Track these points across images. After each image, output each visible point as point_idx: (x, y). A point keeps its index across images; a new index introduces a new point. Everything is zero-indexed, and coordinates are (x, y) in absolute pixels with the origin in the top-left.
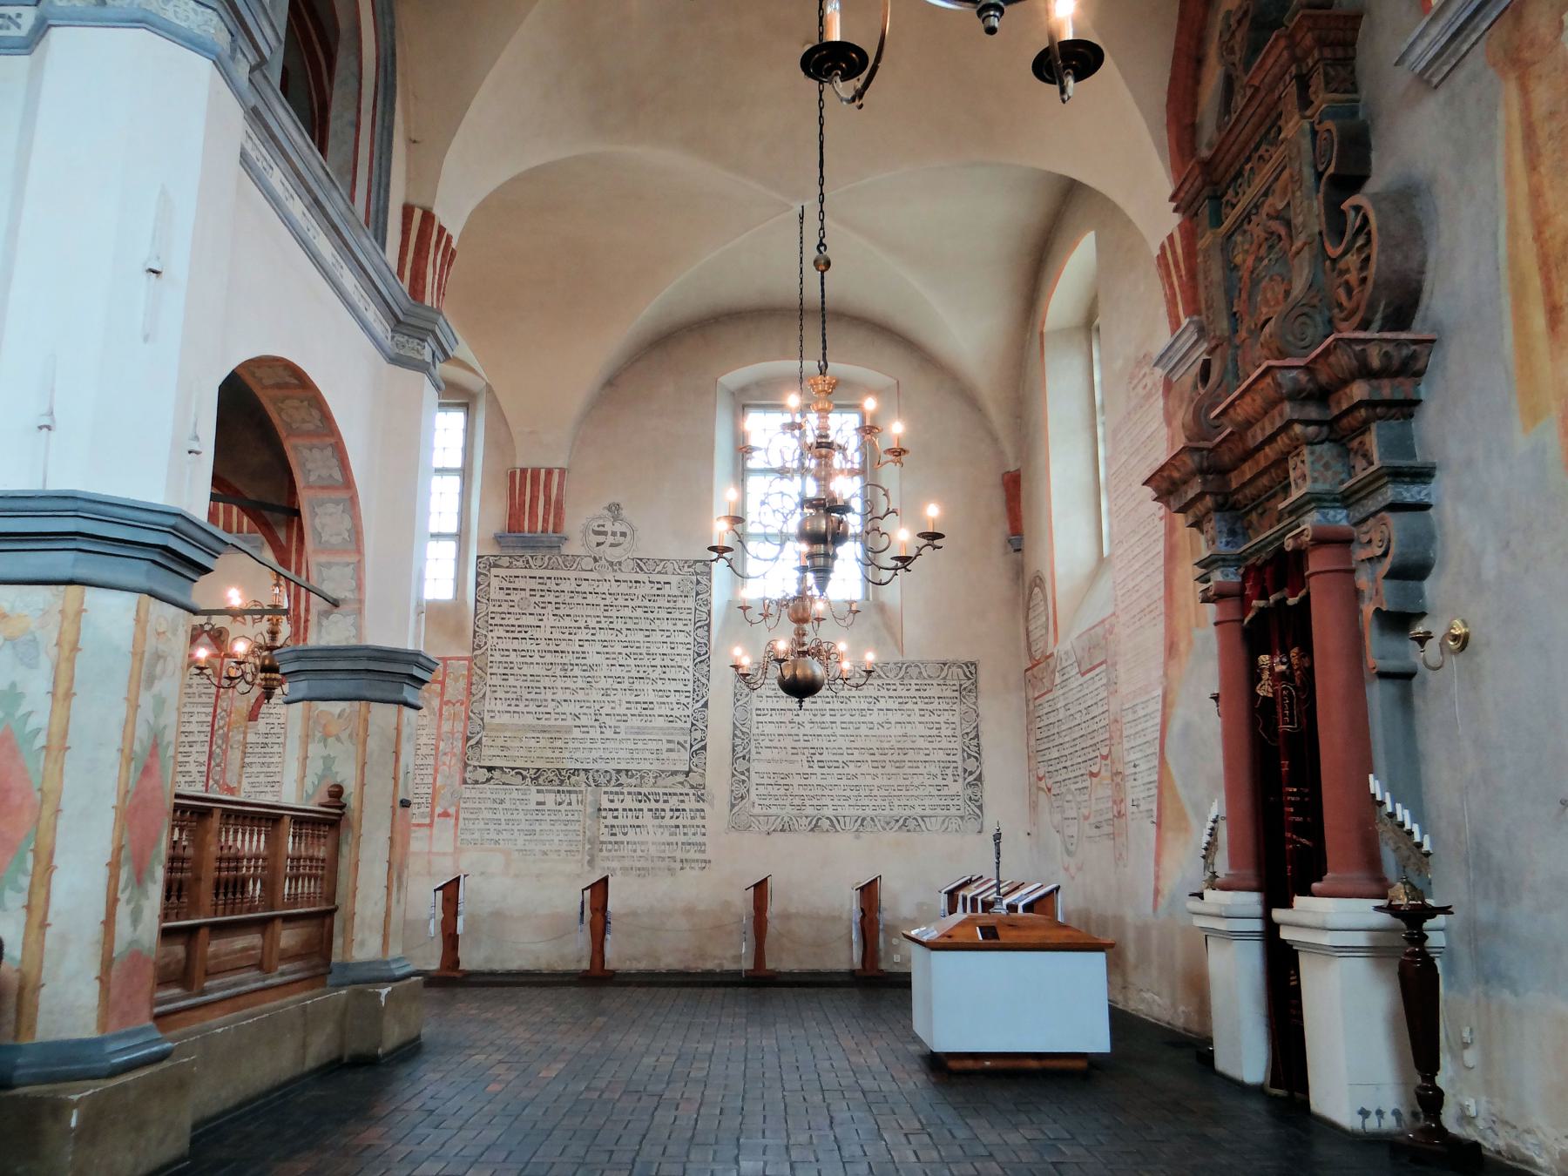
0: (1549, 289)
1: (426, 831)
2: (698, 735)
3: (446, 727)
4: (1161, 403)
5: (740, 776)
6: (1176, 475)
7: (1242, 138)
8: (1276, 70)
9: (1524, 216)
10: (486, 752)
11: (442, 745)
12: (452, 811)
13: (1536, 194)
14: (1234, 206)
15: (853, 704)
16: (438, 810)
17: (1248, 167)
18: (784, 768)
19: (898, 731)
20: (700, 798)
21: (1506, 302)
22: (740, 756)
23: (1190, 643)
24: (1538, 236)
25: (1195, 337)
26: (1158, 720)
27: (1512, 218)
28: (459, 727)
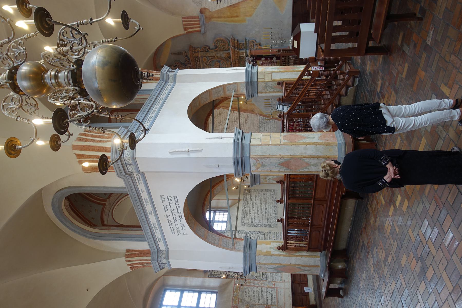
0: (234, 17)
1: (278, 289)
2: (256, 233)
3: (252, 284)
5: (266, 226)
9: (226, 19)
10: (259, 275)
11: (257, 285)
12: (273, 283)
13: (225, 17)
15: (251, 207)
16: (273, 286)
18: (264, 219)
19: (257, 201)
20: (270, 233)
21: (233, 23)
22: (262, 226)
23: (253, 104)
24: (228, 17)
28: (252, 281)
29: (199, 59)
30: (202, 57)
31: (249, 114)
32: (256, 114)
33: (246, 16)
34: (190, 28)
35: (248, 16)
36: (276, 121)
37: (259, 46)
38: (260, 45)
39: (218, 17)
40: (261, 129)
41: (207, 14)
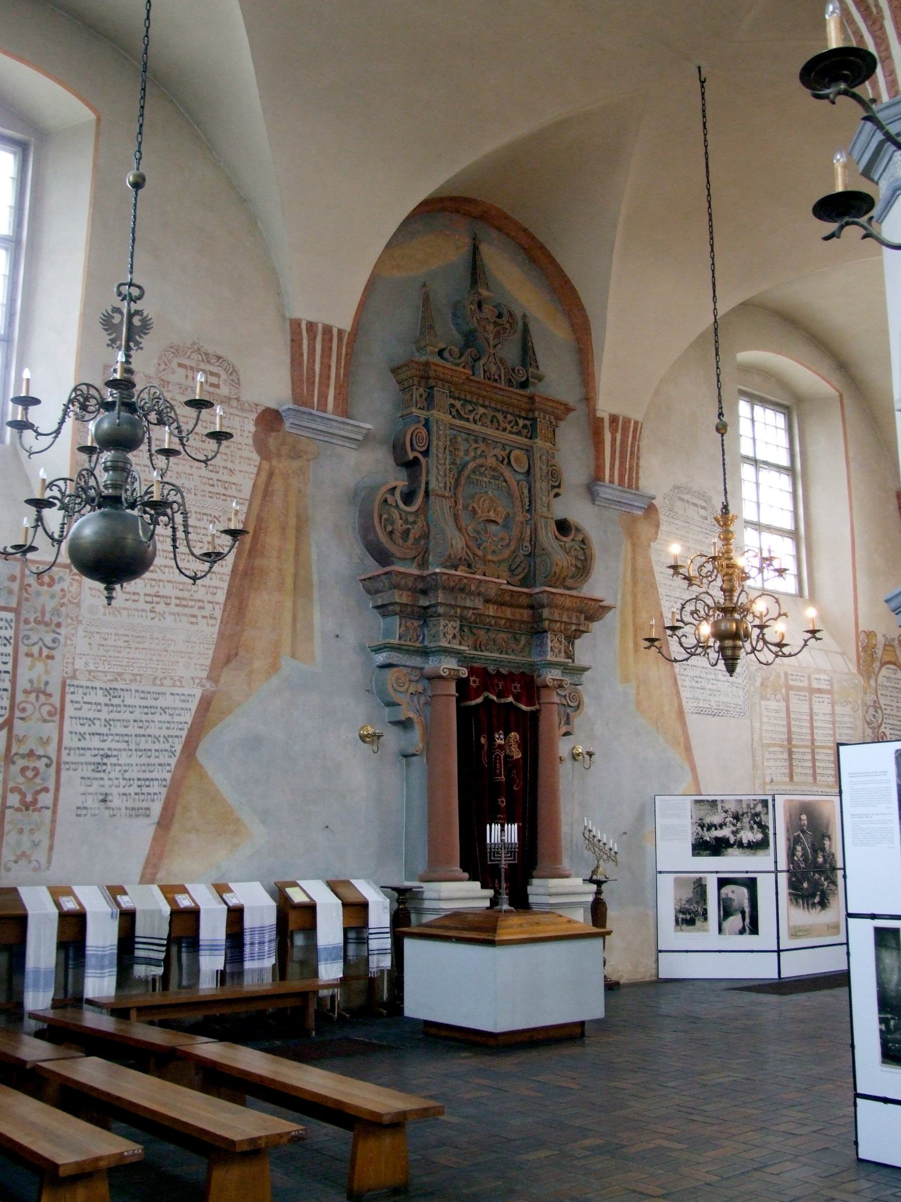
4: (253, 429)
6: (473, 588)
7: (493, 396)
8: (551, 410)
9: (629, 599)
13: (634, 596)
14: (461, 417)
17: (481, 410)
23: (275, 667)
24: (634, 612)
25: (360, 437)
26: (188, 718)
27: (623, 595)
29: (519, 433)
30: (528, 450)
31: (210, 631)
32: (214, 677)
33: (638, 687)
34: (614, 440)
35: (638, 694)
36: (157, 808)
37: (564, 729)
38: (567, 734)
39: (634, 571)
40: (99, 697)
41: (644, 529)
